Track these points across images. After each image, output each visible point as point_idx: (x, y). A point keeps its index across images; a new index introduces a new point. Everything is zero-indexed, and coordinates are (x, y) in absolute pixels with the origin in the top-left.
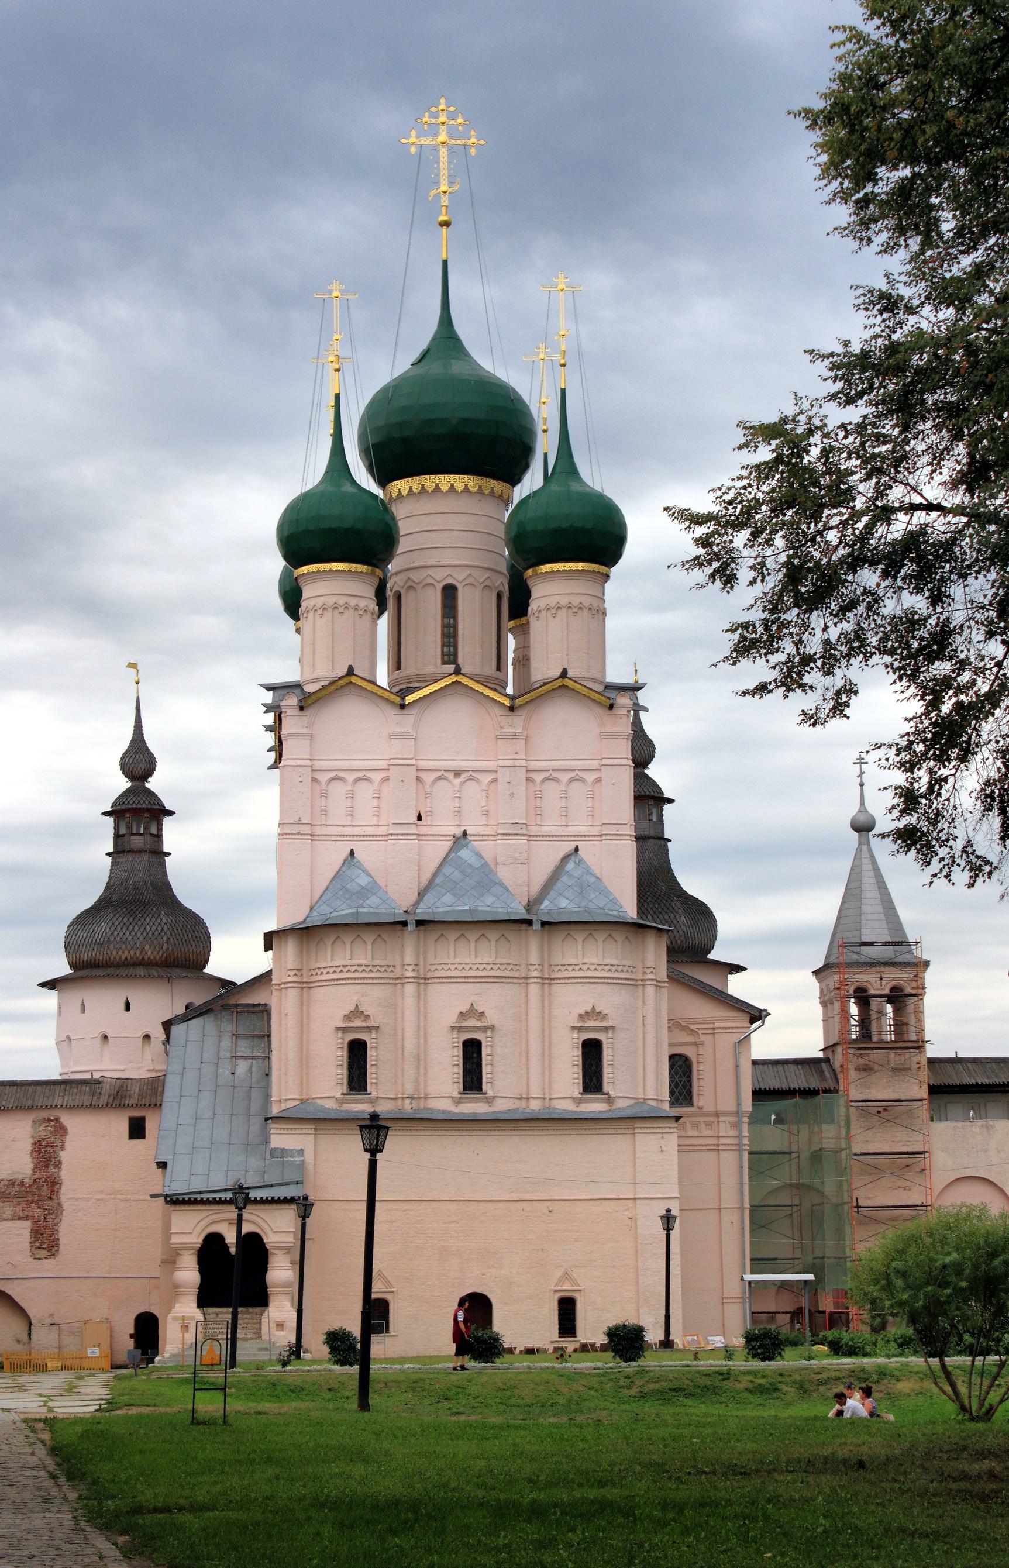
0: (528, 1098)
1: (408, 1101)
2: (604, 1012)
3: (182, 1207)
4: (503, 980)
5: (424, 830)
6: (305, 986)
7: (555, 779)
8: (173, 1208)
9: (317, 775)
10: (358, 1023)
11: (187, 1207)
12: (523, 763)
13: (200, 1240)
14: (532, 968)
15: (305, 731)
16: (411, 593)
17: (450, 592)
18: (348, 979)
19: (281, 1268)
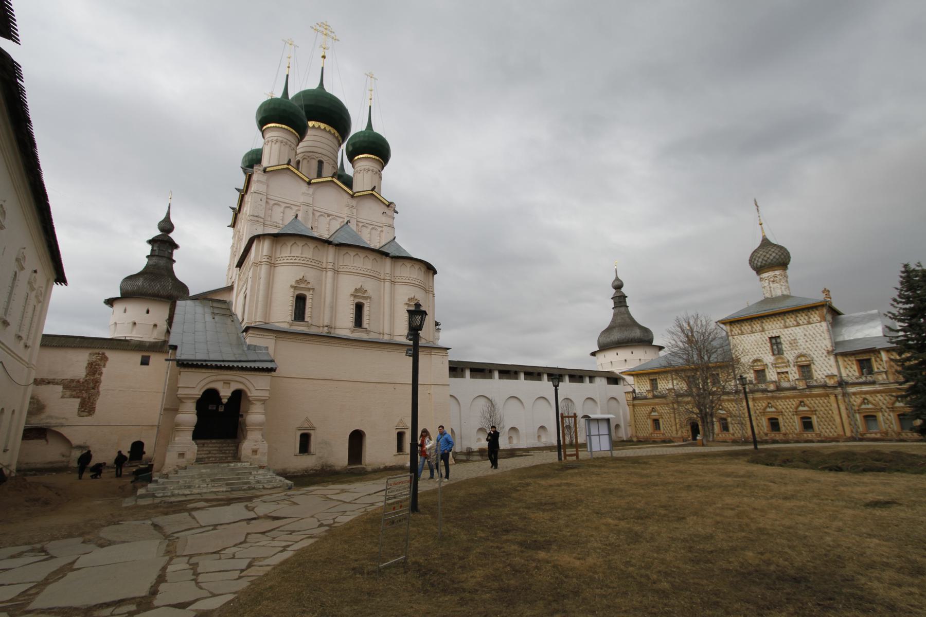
0: (383, 334)
1: (327, 328)
13: (201, 393)
14: (388, 275)
16: (305, 161)
17: (321, 163)
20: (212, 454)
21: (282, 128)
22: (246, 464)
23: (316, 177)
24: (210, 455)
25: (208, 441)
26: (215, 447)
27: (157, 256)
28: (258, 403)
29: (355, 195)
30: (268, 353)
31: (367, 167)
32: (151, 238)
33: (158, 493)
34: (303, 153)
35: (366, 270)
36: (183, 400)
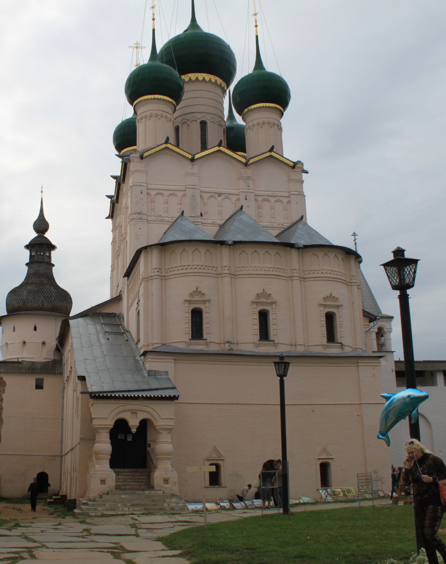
0: (295, 345)
1: (228, 344)
2: (336, 297)
3: (101, 401)
4: (279, 277)
5: (204, 221)
6: (163, 278)
7: (268, 200)
8: (95, 401)
9: (150, 191)
10: (197, 298)
11: (104, 401)
12: (253, 191)
13: (113, 424)
14: (295, 271)
15: (143, 169)
16: (185, 126)
18: (191, 273)
19: (166, 442)
20: (127, 482)
21: (154, 99)
22: (159, 492)
23: (199, 151)
24: (126, 483)
25: (122, 470)
26: (129, 476)
27: (36, 262)
28: (165, 432)
29: (249, 163)
30: (169, 378)
31: (261, 121)
32: (28, 243)
33: (91, 513)
34: (181, 116)
35: (267, 269)
36: (99, 431)
